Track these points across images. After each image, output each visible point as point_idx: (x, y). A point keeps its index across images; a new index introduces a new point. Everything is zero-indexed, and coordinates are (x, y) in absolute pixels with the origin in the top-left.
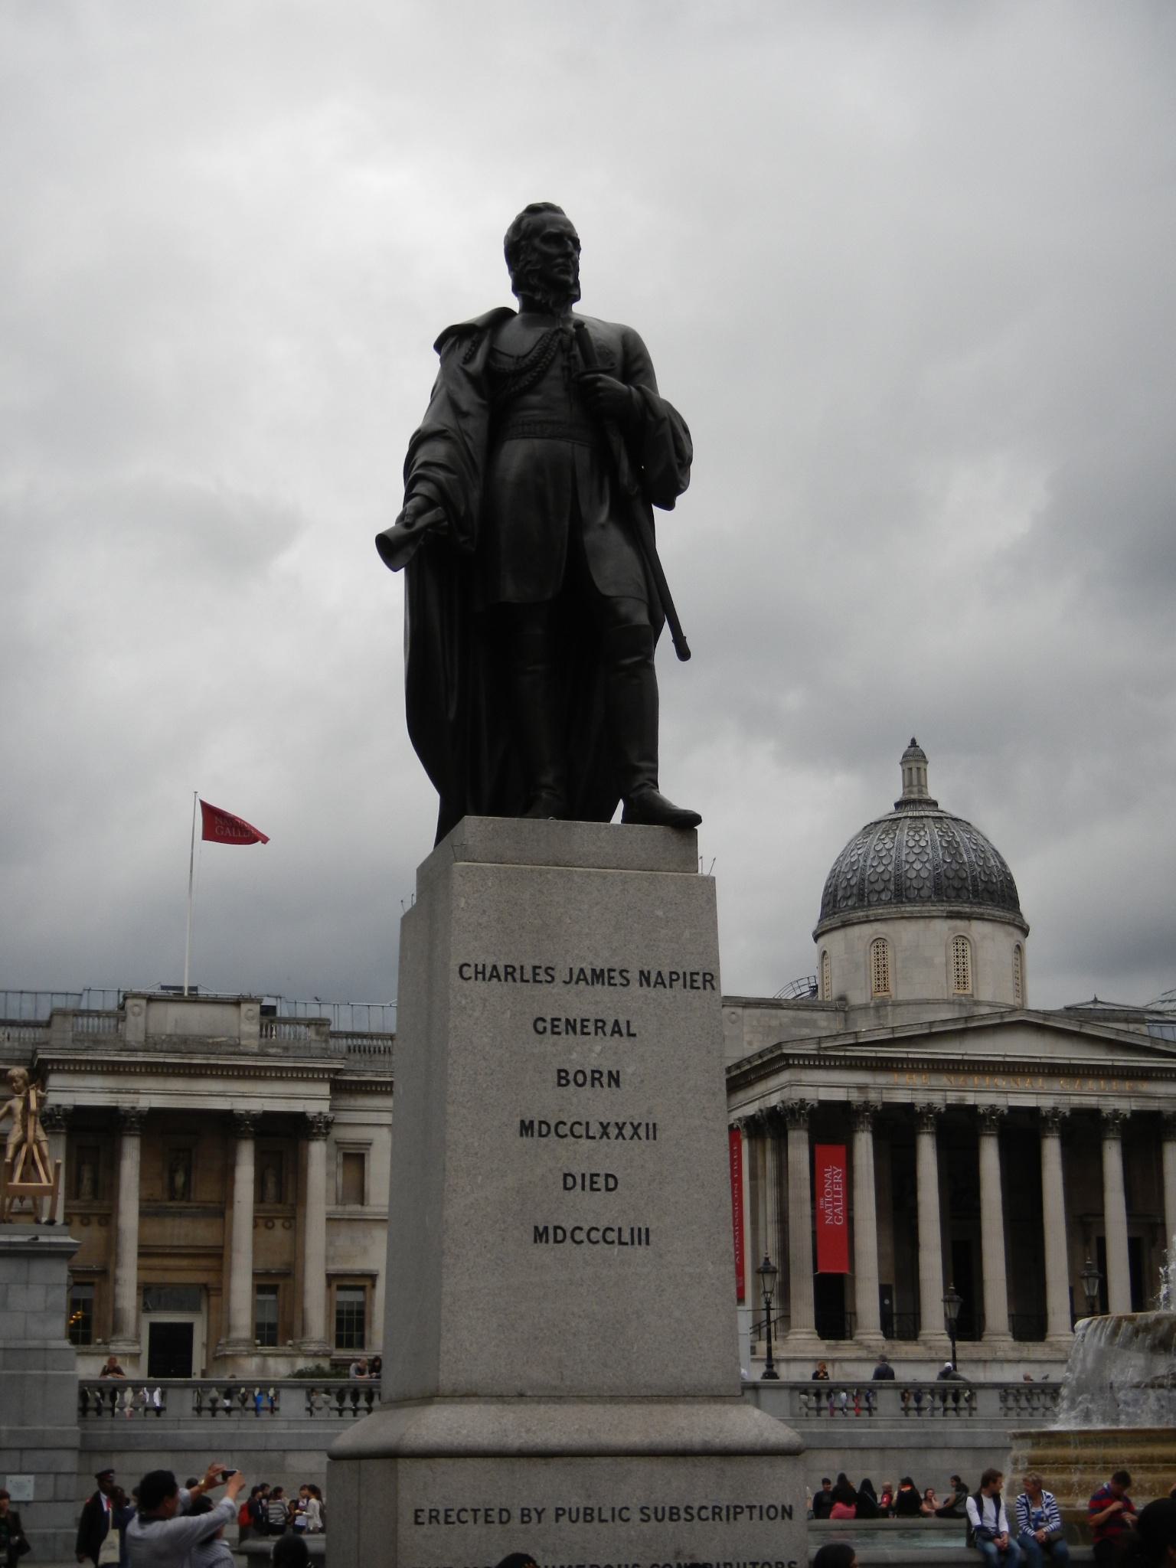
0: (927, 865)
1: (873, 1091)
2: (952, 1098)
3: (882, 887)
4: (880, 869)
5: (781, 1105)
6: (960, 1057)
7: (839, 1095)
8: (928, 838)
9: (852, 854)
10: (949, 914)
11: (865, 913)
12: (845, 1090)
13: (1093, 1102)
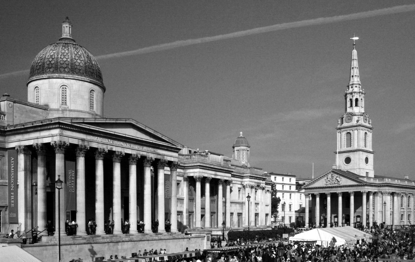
0: (82, 61)
1: (86, 142)
2: (109, 147)
3: (66, 66)
4: (65, 59)
5: (53, 143)
6: (114, 133)
7: (75, 142)
8: (81, 53)
9: (50, 52)
10: (90, 81)
11: (59, 75)
12: (78, 140)
13: (145, 154)
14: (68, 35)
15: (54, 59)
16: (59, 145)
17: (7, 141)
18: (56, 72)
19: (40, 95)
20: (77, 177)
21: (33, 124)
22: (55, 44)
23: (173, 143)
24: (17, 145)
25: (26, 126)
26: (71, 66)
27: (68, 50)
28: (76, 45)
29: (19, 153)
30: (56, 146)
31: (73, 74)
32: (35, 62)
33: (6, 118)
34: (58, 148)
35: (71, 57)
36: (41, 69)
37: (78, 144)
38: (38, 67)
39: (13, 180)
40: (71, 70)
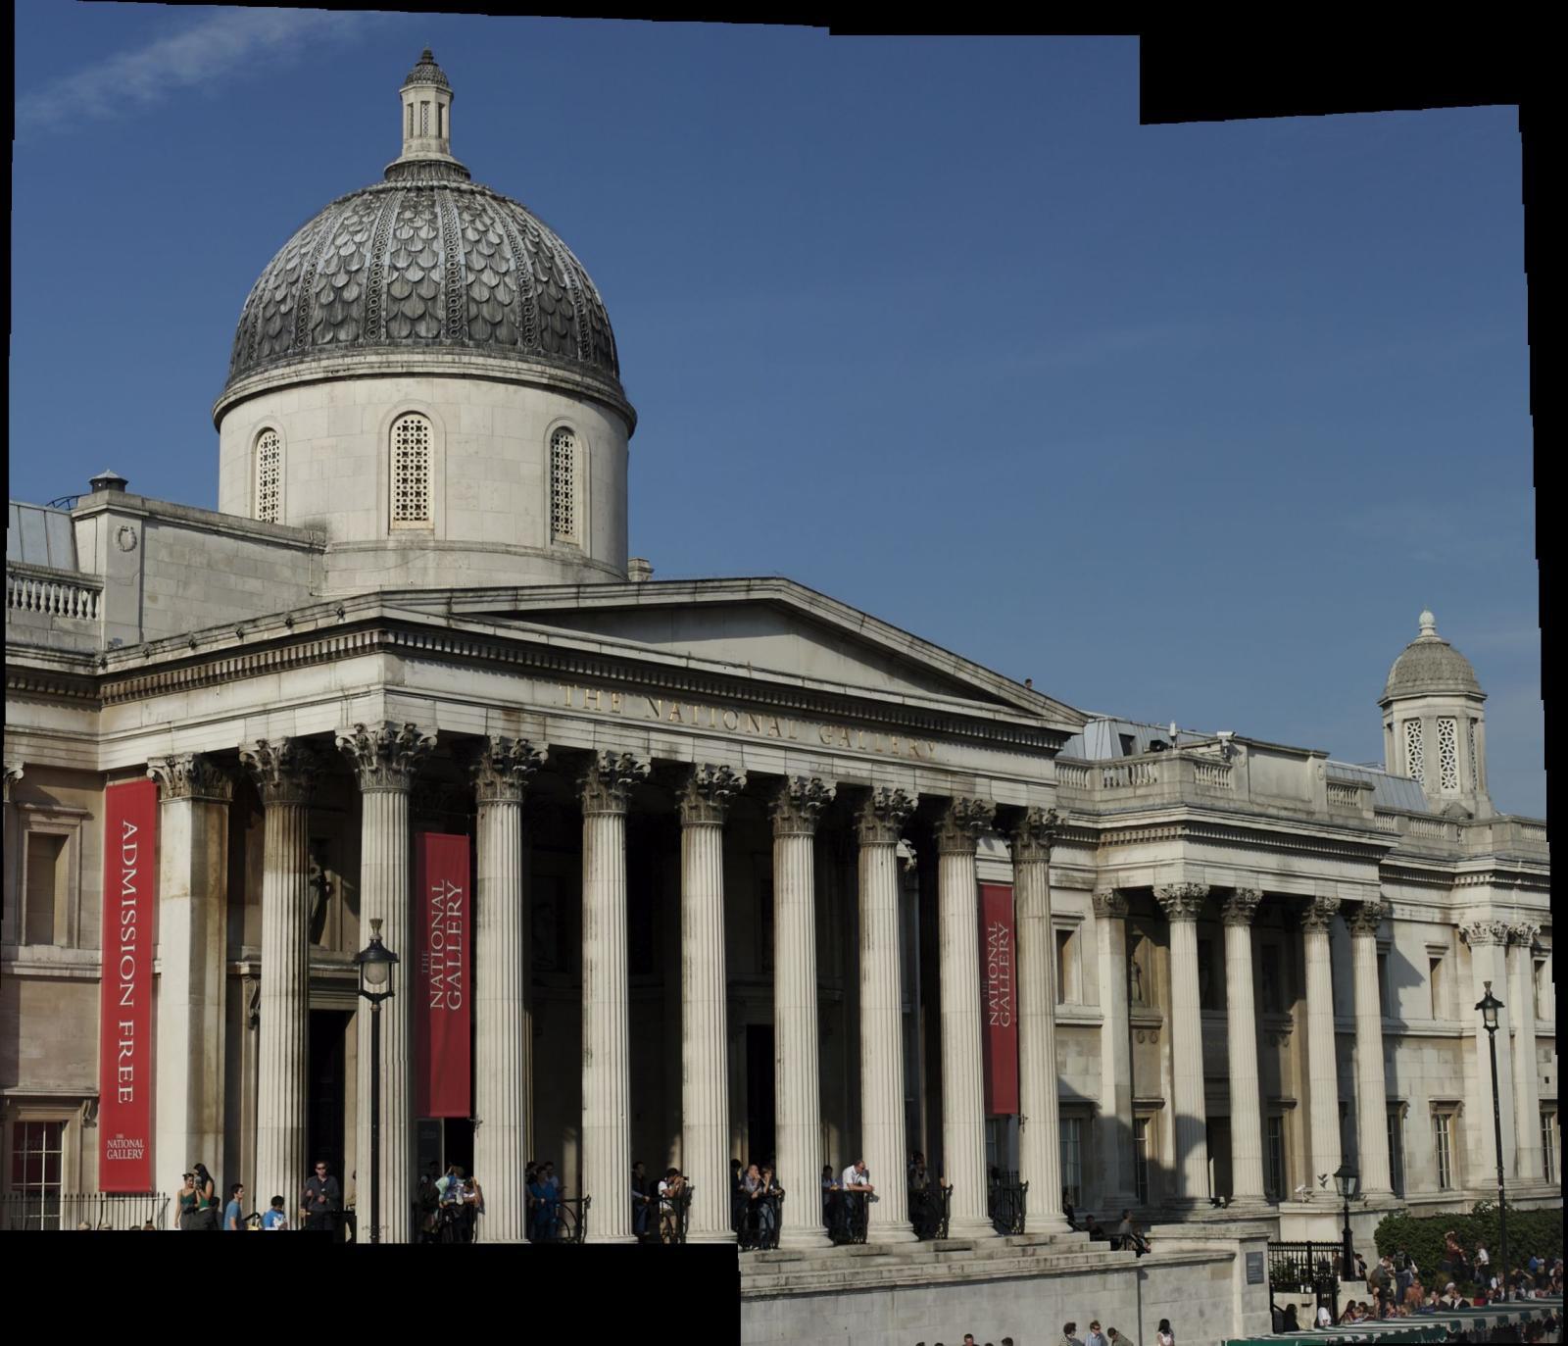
0: (507, 279)
1: (528, 718)
2: (660, 745)
4: (414, 275)
5: (346, 734)
6: (682, 663)
7: (468, 722)
8: (500, 230)
9: (339, 242)
10: (552, 382)
11: (384, 358)
12: (482, 711)
13: (865, 774)
14: (434, 143)
15: (360, 274)
16: (381, 747)
17: (103, 735)
18: (368, 345)
19: (281, 471)
20: (480, 919)
21: (241, 636)
22: (366, 196)
23: (1025, 704)
24: (159, 755)
25: (203, 649)
26: (448, 309)
27: (432, 222)
28: (472, 192)
29: (163, 796)
30: (362, 748)
31: (457, 349)
32: (261, 298)
33: (101, 608)
34: (374, 759)
35: (449, 258)
36: (290, 332)
37: (483, 733)
38: (277, 324)
39: (132, 948)
40: (448, 330)
